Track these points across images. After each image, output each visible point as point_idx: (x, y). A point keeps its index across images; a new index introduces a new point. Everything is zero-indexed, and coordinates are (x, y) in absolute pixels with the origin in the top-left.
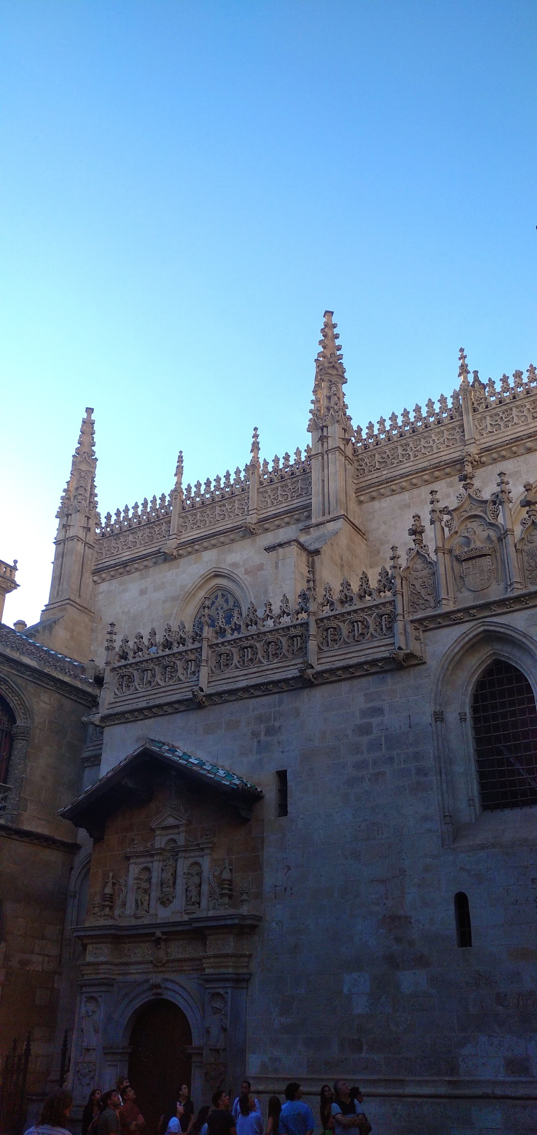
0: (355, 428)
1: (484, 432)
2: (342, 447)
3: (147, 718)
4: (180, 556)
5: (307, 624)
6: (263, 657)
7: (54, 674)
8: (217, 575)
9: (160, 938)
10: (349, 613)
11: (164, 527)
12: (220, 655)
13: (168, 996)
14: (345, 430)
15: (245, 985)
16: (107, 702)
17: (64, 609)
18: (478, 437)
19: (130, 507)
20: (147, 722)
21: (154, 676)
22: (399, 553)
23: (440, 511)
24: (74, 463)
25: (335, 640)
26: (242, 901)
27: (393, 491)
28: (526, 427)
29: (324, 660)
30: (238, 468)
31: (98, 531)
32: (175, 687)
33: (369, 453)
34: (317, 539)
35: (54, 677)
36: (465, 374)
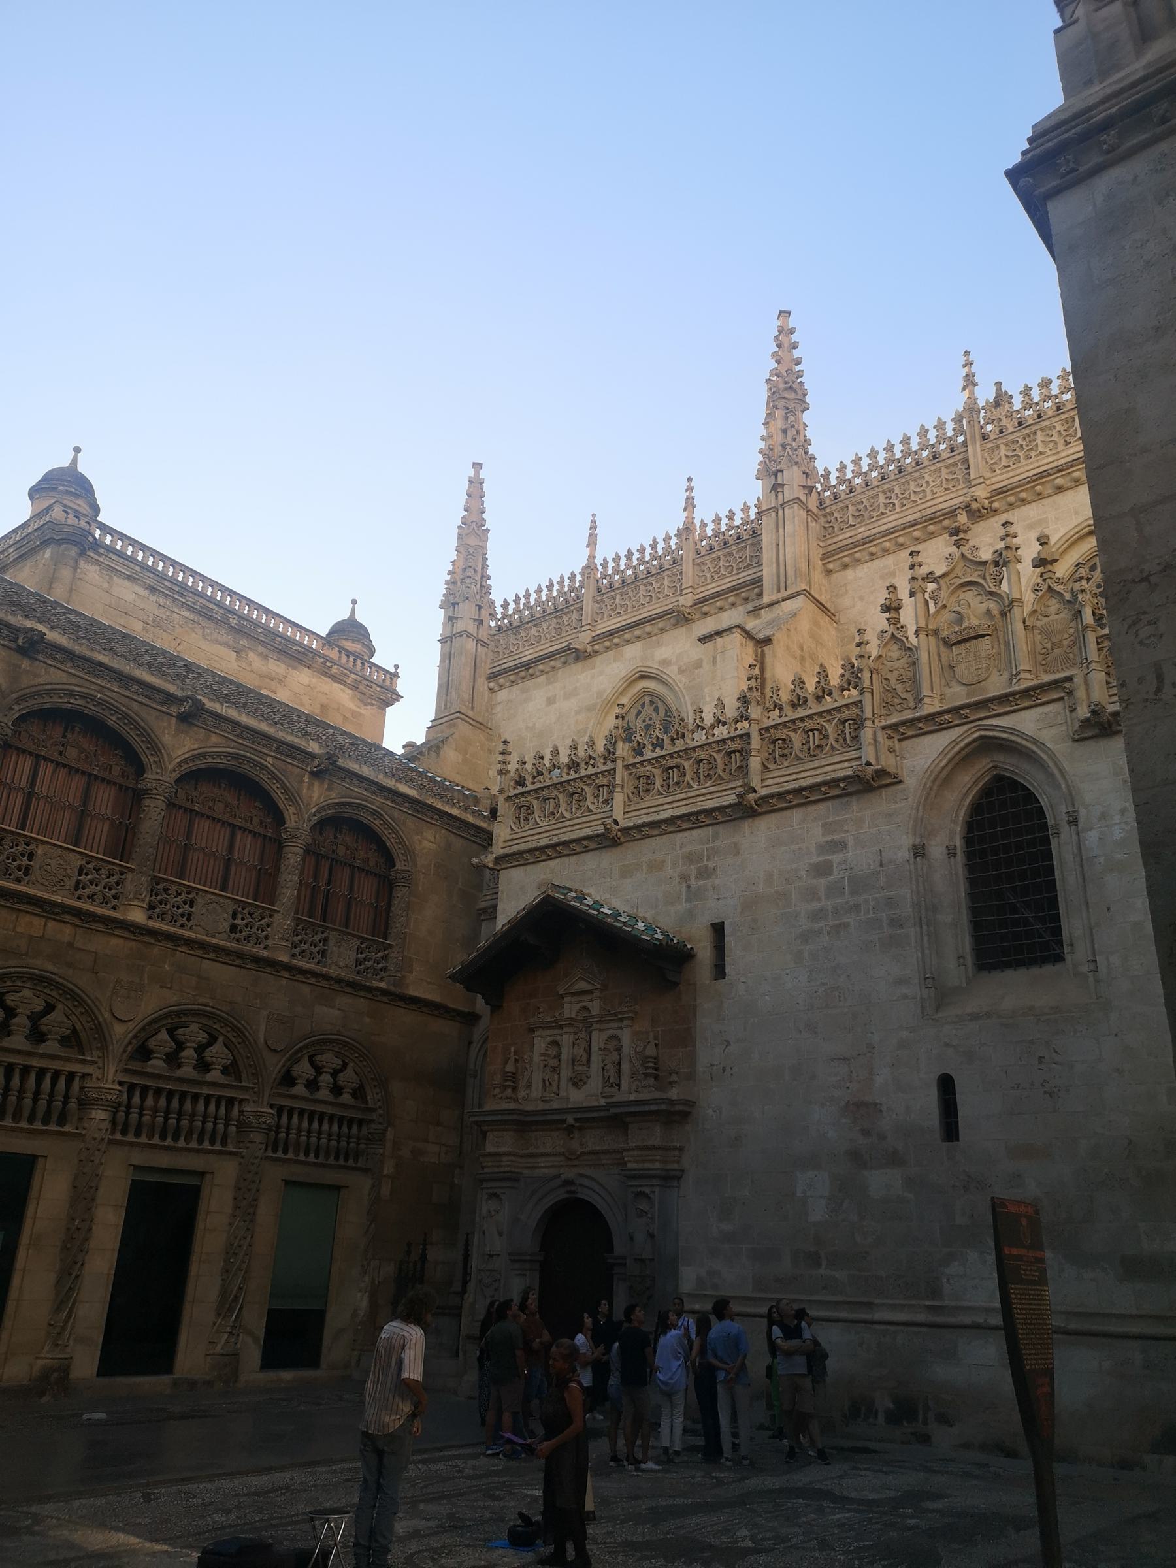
0: (821, 472)
1: (996, 467)
2: (803, 498)
4: (596, 652)
5: (748, 735)
7: (440, 806)
8: (643, 677)
9: (573, 1126)
10: (802, 719)
11: (575, 616)
12: (639, 778)
13: (583, 1194)
14: (807, 475)
15: (675, 1183)
16: (501, 839)
17: (454, 725)
18: (988, 475)
19: (531, 592)
20: (552, 863)
21: (558, 806)
22: (866, 637)
23: (923, 579)
24: (460, 537)
25: (784, 756)
26: (671, 1083)
27: (872, 554)
28: (1055, 458)
29: (770, 782)
30: (667, 534)
31: (493, 624)
32: (584, 820)
33: (841, 505)
34: (769, 623)
35: (439, 810)
36: (971, 387)
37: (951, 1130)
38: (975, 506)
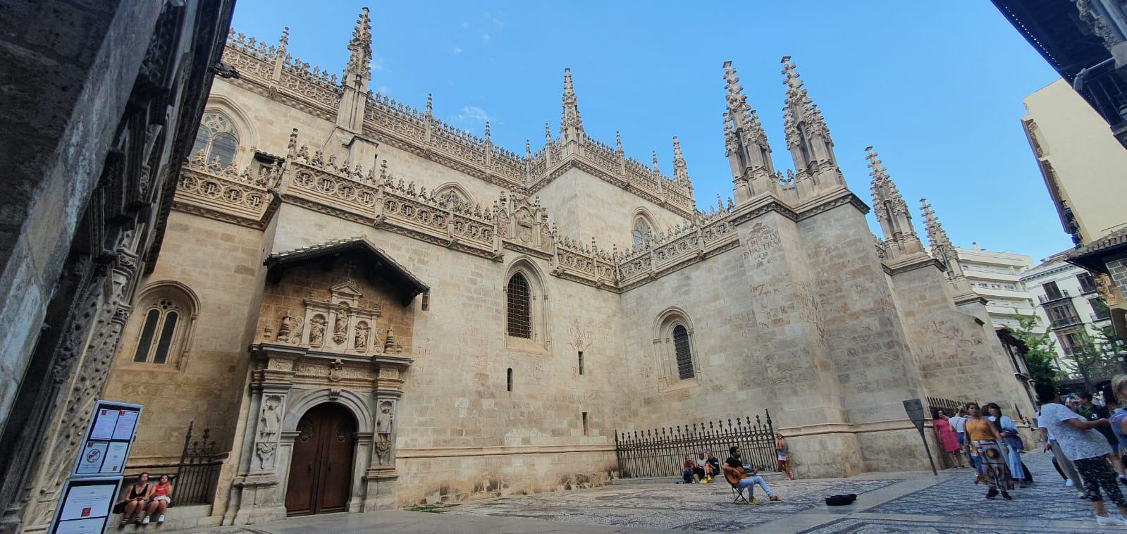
3: (328, 214)
5: (448, 214)
9: (338, 363)
10: (471, 220)
12: (389, 202)
37: (509, 388)
38: (428, 152)
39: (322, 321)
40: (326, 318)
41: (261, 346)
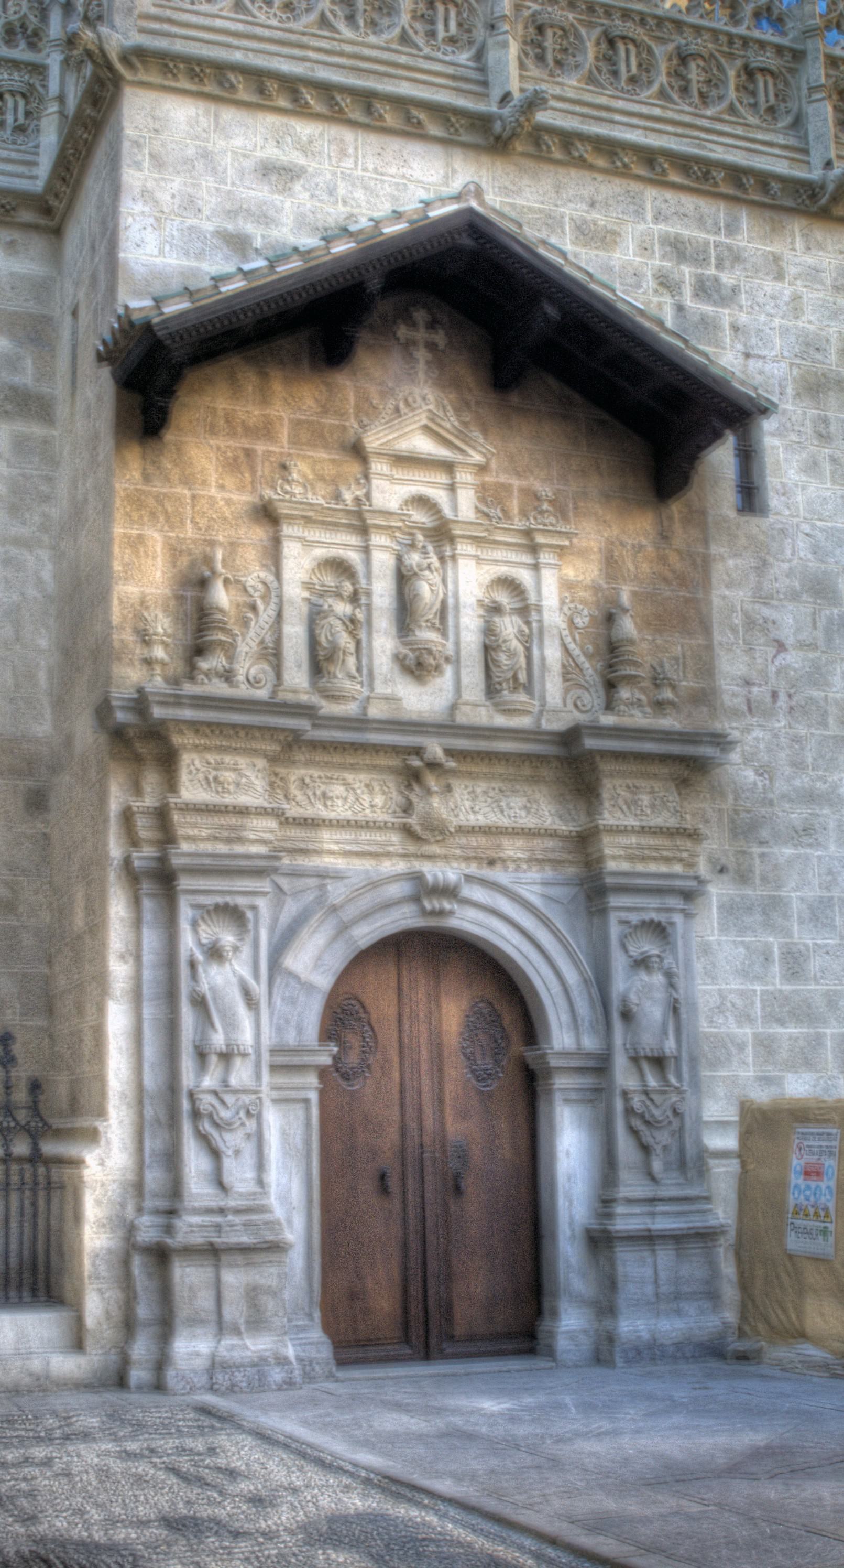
6: (672, 88)
9: (433, 766)
12: (540, 29)
39: (348, 587)
40: (360, 569)
41: (140, 703)
